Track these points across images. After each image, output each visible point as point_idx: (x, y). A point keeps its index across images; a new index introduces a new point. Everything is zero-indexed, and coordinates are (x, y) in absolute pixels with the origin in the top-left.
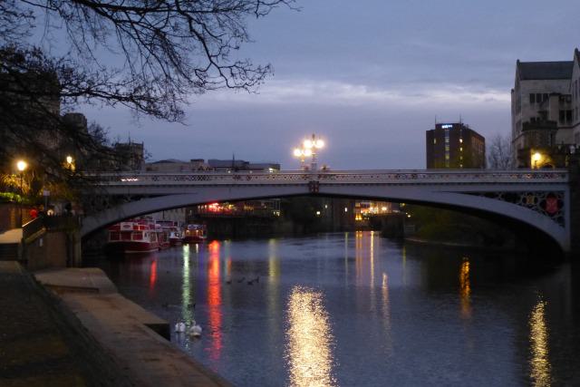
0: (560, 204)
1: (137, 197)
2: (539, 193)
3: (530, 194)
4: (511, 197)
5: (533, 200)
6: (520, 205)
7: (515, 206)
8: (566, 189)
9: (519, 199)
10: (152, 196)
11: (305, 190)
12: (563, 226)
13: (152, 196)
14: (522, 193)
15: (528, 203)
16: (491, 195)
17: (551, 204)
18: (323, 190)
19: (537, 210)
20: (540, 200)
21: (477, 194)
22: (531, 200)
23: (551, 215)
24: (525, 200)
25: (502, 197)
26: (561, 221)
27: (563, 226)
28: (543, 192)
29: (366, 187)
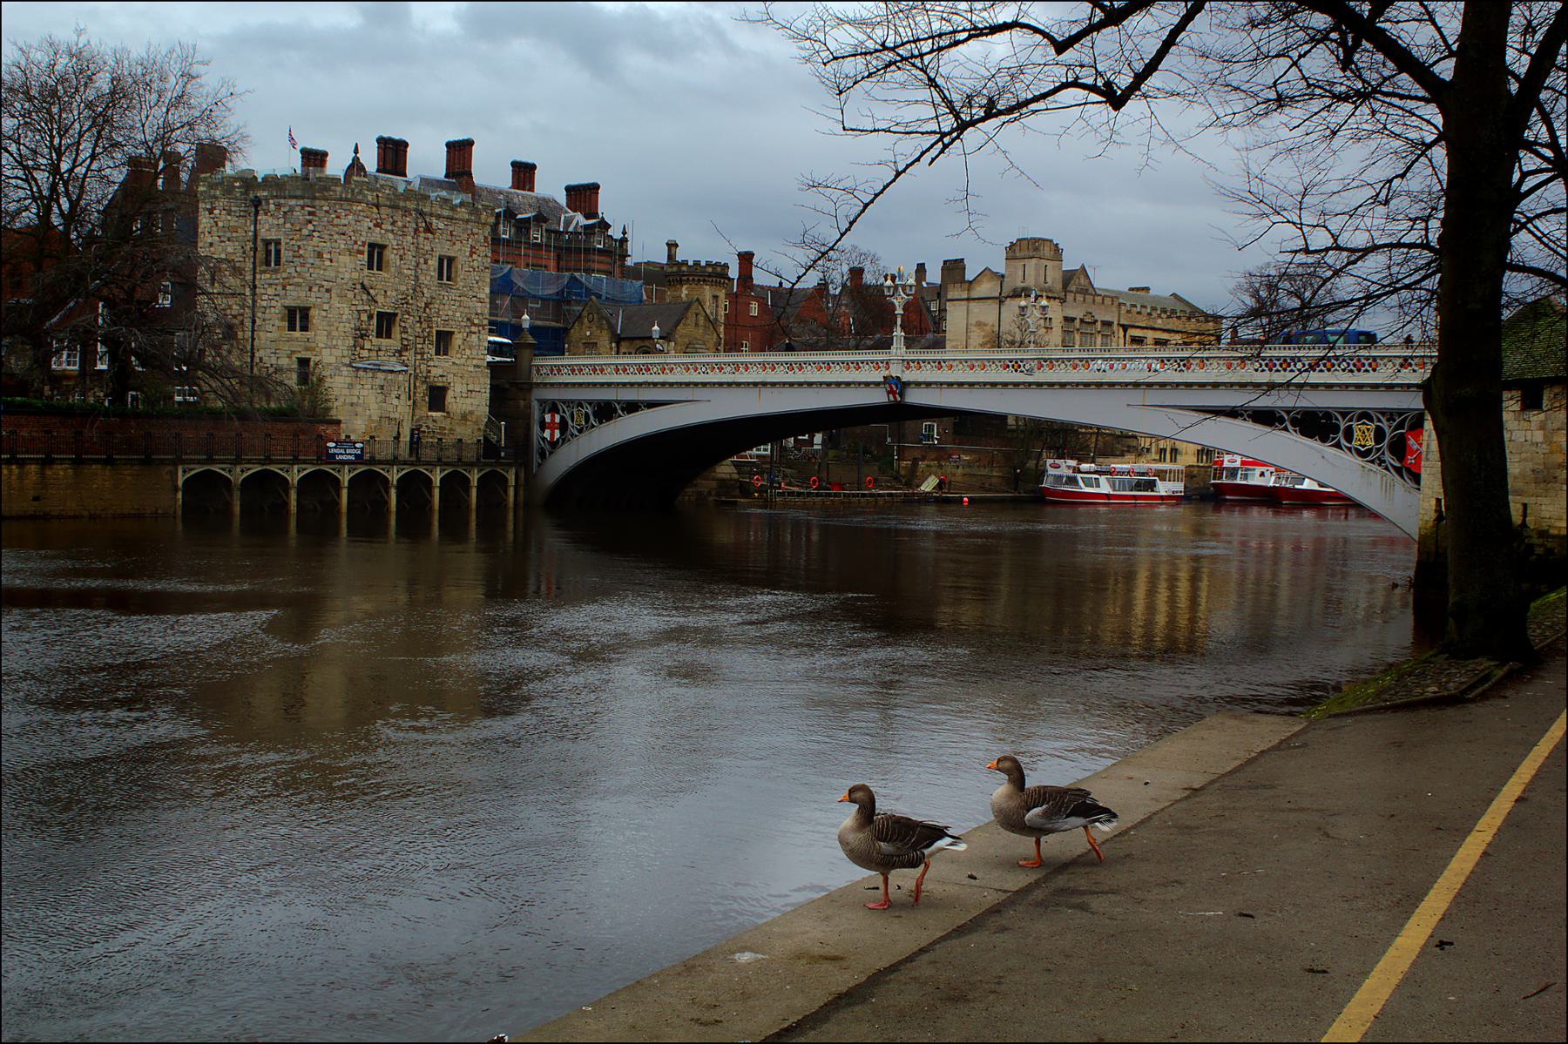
1: (632, 407)
2: (1390, 414)
3: (1365, 415)
4: (1316, 425)
5: (1357, 434)
6: (1338, 446)
7: (1328, 450)
9: (1336, 429)
11: (879, 397)
14: (1344, 413)
15: (1355, 444)
16: (1266, 418)
18: (915, 397)
19: (1381, 462)
21: (1233, 413)
25: (1294, 422)
28: (1400, 412)
29: (995, 392)
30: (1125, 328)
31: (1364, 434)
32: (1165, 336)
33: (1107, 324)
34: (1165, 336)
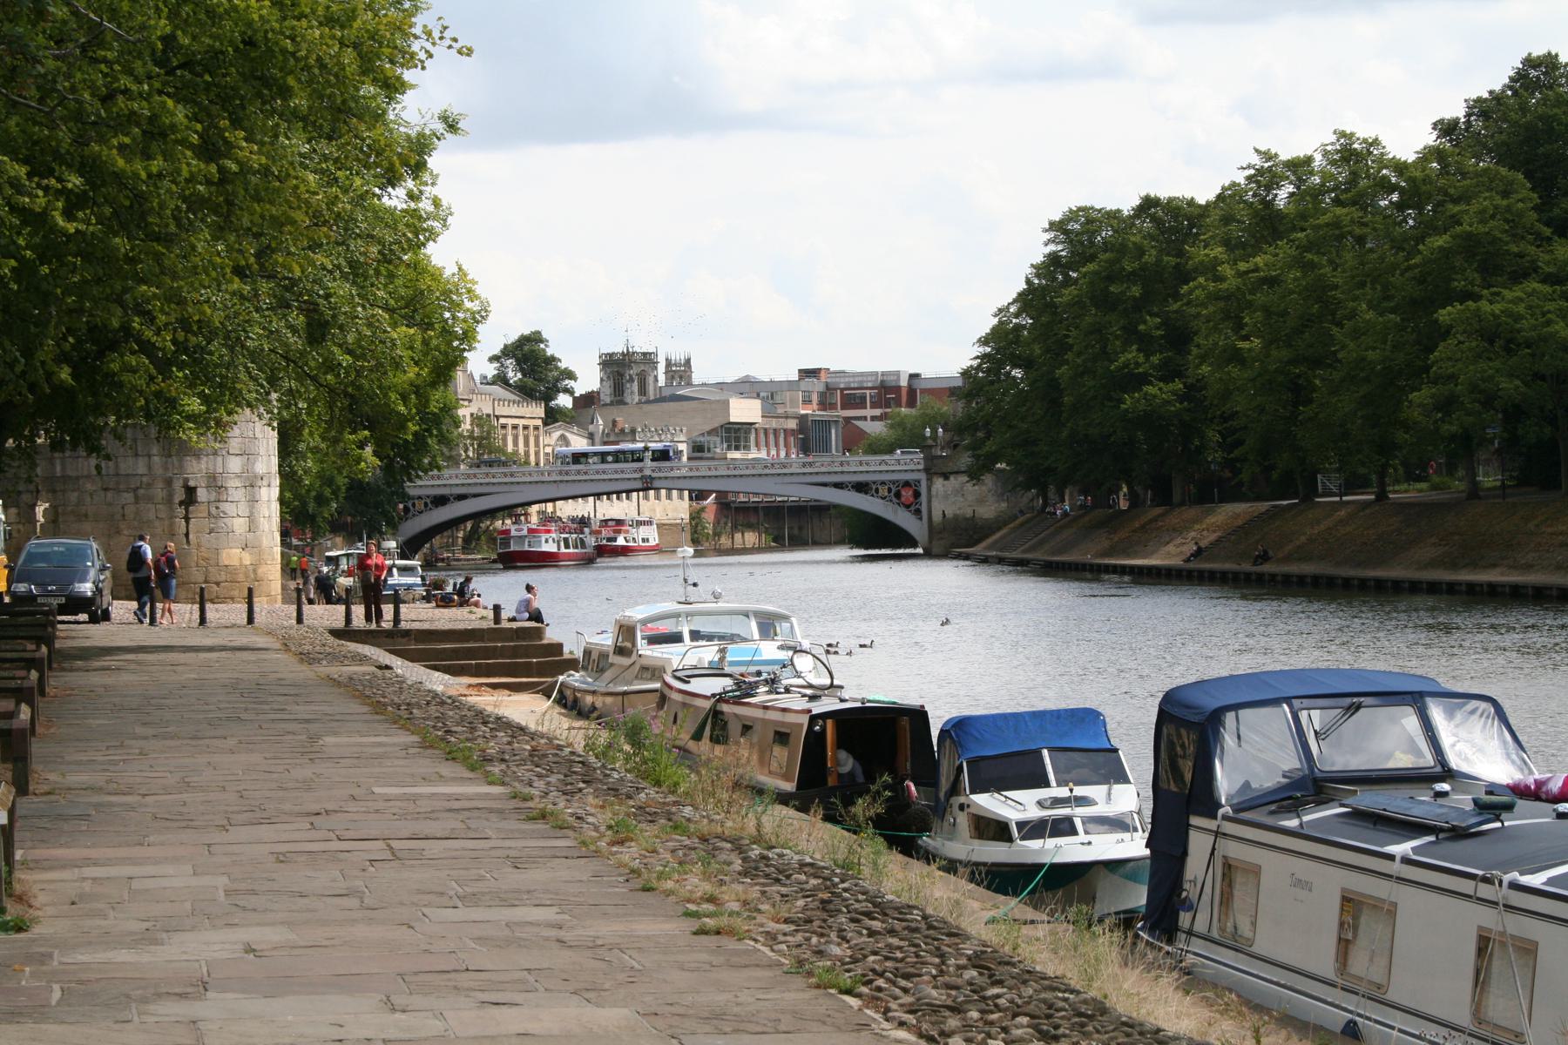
0: (917, 495)
2: (894, 482)
3: (883, 483)
4: (861, 487)
8: (923, 477)
10: (475, 496)
12: (921, 519)
13: (475, 496)
16: (838, 485)
17: (907, 494)
20: (894, 490)
21: (825, 485)
22: (883, 491)
23: (907, 507)
24: (877, 491)
26: (918, 512)
27: (921, 519)
30: (498, 417)
31: (883, 491)
32: (516, 421)
33: (488, 415)
34: (516, 421)
